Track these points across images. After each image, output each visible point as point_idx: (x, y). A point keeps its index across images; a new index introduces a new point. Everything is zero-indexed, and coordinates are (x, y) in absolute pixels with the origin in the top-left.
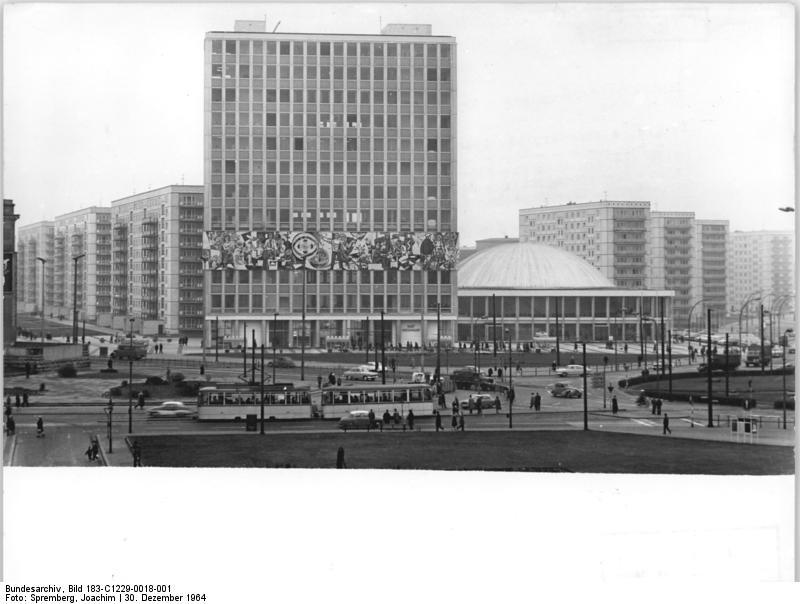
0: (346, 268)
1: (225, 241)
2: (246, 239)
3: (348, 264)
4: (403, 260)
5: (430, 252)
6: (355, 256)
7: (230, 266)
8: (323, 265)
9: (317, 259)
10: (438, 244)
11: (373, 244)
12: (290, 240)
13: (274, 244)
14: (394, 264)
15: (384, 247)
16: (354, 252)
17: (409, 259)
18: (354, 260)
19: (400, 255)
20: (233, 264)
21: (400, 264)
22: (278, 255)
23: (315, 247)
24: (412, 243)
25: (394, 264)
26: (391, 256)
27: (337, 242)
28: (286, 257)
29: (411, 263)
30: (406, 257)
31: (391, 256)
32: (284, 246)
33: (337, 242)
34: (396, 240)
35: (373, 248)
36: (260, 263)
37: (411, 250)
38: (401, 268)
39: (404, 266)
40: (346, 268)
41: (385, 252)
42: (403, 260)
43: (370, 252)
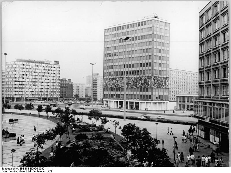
2: (110, 80)
4: (140, 85)
5: (146, 82)
6: (130, 84)
10: (148, 80)
13: (115, 81)
14: (138, 86)
16: (130, 83)
17: (141, 84)
18: (130, 85)
19: (139, 83)
21: (139, 86)
24: (142, 80)
25: (138, 86)
28: (117, 84)
30: (140, 84)
31: (137, 84)
36: (112, 86)
38: (140, 87)
41: (136, 82)
42: (140, 85)
43: (133, 83)
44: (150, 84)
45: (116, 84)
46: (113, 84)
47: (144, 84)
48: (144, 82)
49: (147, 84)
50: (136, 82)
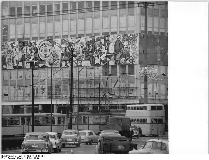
4: (103, 57)
10: (125, 43)
11: (85, 46)
17: (107, 56)
21: (101, 61)
22: (30, 58)
25: (97, 61)
26: (96, 55)
28: (36, 59)
29: (108, 59)
30: (105, 55)
31: (96, 55)
34: (99, 42)
35: (85, 49)
38: (102, 64)
41: (92, 52)
42: (103, 57)
43: (83, 52)
44: (131, 54)
45: (32, 57)
46: (23, 59)
47: (115, 55)
48: (115, 50)
49: (122, 56)
50: (92, 52)
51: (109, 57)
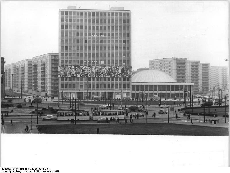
0: (100, 77)
1: (65, 69)
3: (100, 76)
4: (116, 74)
5: (124, 72)
6: (102, 73)
7: (66, 76)
8: (93, 76)
9: (91, 74)
10: (126, 70)
11: (107, 70)
12: (84, 69)
13: (79, 70)
14: (113, 76)
15: (110, 71)
16: (102, 72)
17: (118, 74)
18: (102, 74)
19: (115, 73)
20: (67, 76)
21: (115, 76)
23: (91, 71)
24: (119, 70)
25: (113, 76)
26: (113, 73)
27: (97, 69)
29: (118, 75)
30: (117, 74)
31: (113, 73)
32: (82, 71)
33: (97, 69)
34: (114, 69)
35: (107, 71)
36: (75, 75)
37: (118, 72)
38: (115, 77)
39: (116, 76)
40: (100, 77)
41: (111, 72)
43: (106, 72)
51: (119, 75)
